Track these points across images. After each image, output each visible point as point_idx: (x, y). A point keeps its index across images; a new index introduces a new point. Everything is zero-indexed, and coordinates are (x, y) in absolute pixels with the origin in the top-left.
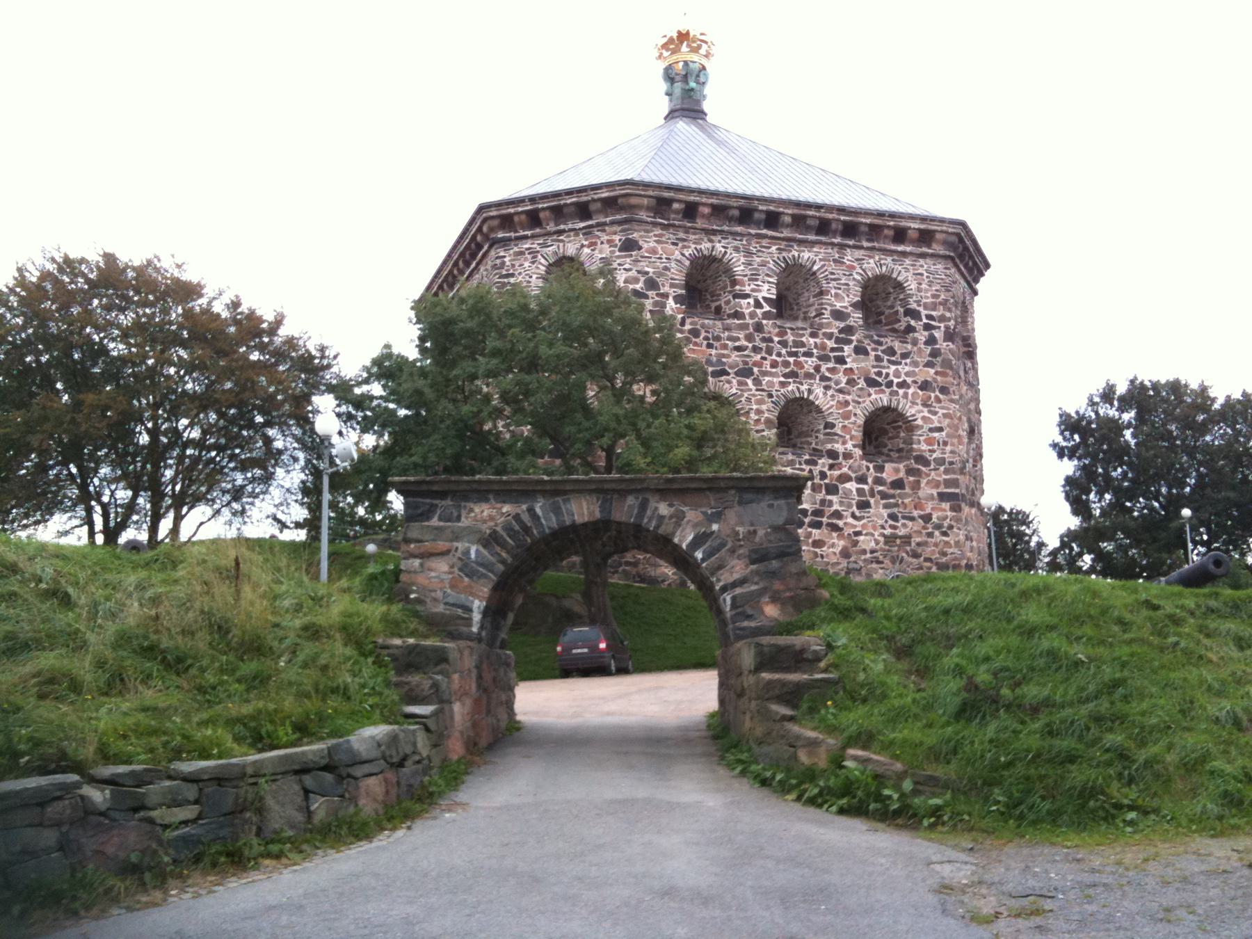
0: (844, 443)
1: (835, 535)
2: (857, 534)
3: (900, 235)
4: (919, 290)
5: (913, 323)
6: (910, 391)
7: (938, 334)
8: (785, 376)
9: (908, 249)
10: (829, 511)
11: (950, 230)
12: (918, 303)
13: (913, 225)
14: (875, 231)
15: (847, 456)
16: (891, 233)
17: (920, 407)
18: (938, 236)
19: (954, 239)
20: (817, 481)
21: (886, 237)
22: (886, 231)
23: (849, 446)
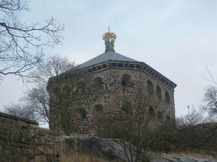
0: (89, 115)
1: (86, 134)
2: (90, 133)
3: (99, 68)
4: (104, 78)
5: (103, 85)
6: (102, 100)
7: (108, 86)
8: (78, 105)
9: (101, 70)
10: (85, 130)
11: (108, 63)
12: (104, 80)
13: (100, 65)
14: (94, 69)
15: (89, 117)
16: (97, 68)
17: (104, 102)
18: (106, 65)
19: (109, 64)
20: (83, 124)
21: (97, 69)
22: (96, 68)
23: (90, 115)
